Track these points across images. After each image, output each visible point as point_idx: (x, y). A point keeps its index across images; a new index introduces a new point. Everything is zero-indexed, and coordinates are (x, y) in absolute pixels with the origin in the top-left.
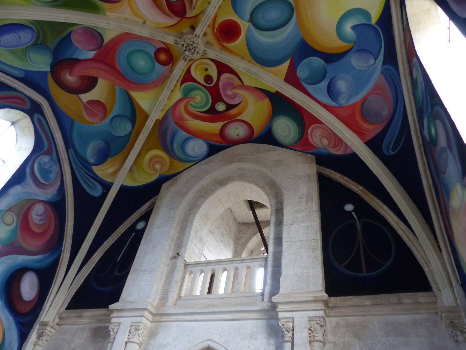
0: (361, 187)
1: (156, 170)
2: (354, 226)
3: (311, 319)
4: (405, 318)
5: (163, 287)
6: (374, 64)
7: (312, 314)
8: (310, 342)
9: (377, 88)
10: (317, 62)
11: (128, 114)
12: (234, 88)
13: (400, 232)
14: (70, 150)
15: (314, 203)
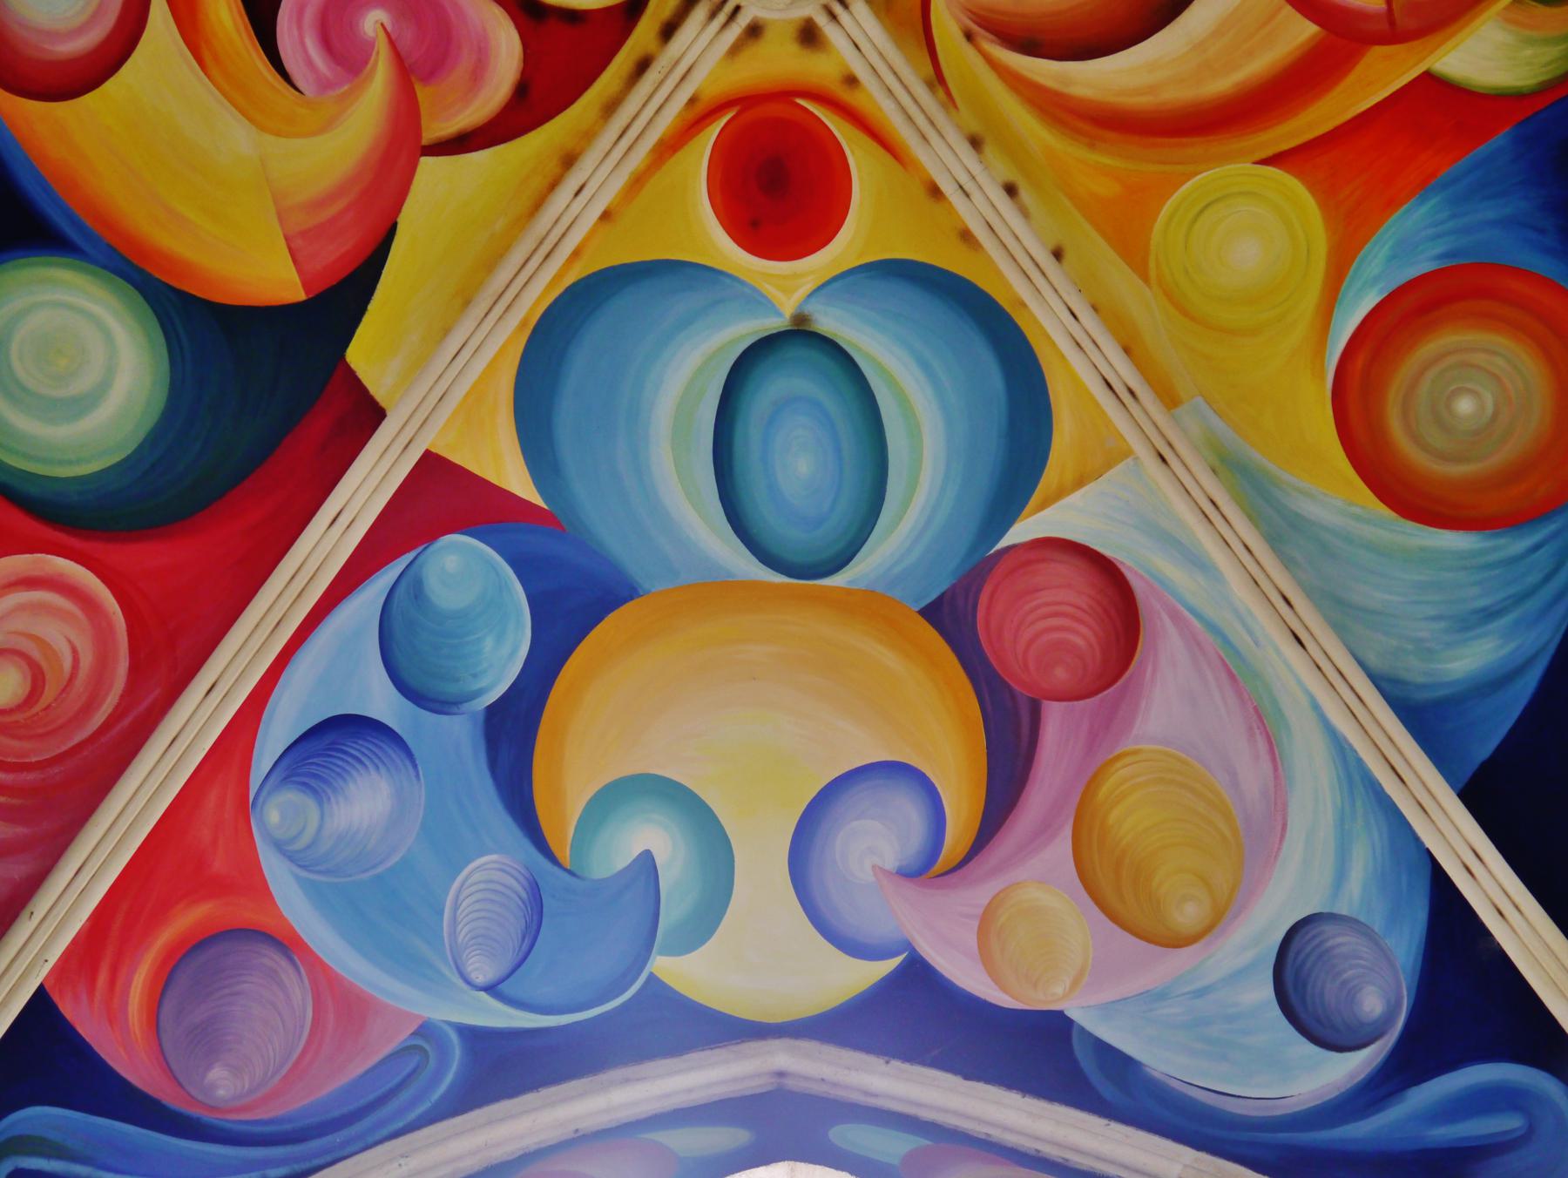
6: (468, 982)
9: (342, 1006)
12: (408, 73)
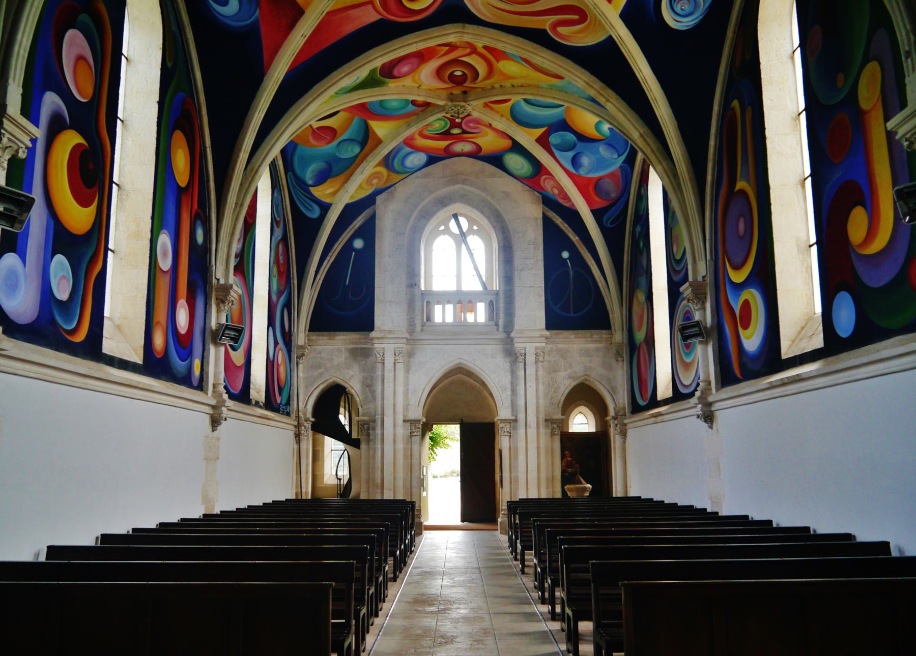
1: (372, 185)
2: (568, 273)
3: (536, 348)
4: (592, 346)
7: (538, 345)
9: (612, 175)
10: (570, 137)
11: (360, 139)
13: (600, 285)
14: (290, 173)
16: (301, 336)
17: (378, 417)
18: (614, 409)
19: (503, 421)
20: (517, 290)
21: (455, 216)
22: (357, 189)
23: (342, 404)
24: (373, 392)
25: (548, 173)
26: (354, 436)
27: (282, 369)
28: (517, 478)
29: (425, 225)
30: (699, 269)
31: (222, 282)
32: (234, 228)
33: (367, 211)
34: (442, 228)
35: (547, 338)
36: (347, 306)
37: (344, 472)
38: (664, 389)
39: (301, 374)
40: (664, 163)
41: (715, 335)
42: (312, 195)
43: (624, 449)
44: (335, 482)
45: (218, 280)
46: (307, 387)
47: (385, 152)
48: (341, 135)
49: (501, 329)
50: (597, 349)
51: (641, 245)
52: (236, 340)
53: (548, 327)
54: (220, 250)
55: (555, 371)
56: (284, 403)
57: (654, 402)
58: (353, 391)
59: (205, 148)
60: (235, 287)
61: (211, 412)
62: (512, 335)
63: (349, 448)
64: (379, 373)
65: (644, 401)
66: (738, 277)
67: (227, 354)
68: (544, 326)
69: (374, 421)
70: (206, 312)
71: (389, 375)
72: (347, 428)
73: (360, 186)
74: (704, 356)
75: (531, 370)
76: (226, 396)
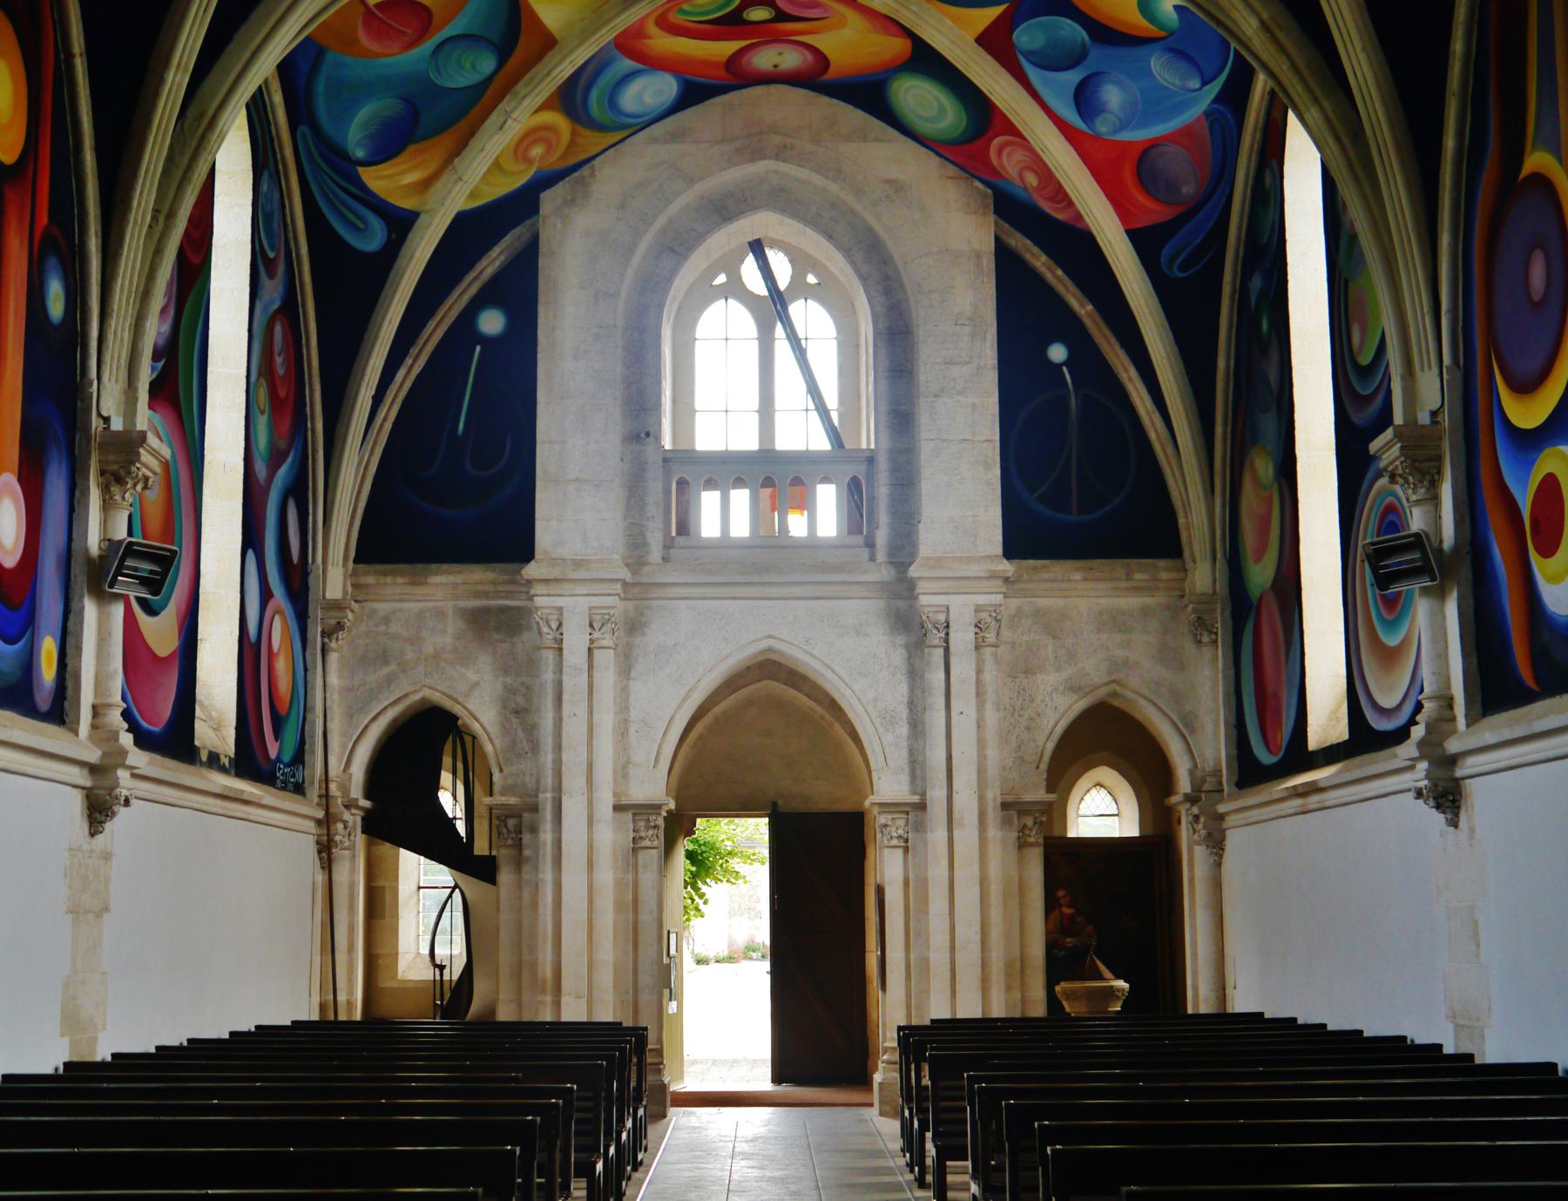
0: (1090, 307)
1: (528, 161)
5: (625, 517)
7: (982, 599)
8: (977, 648)
9: (1184, 136)
10: (1071, 30)
13: (1152, 436)
14: (303, 129)
15: (988, 344)
16: (333, 577)
17: (547, 797)
18: (1192, 773)
19: (886, 807)
20: (926, 450)
21: (757, 248)
22: (489, 171)
23: (447, 760)
24: (531, 730)
25: (1012, 130)
26: (481, 848)
27: (281, 666)
28: (925, 963)
29: (673, 272)
30: (1423, 391)
31: (117, 425)
32: (150, 278)
33: (518, 230)
34: (721, 279)
35: (1006, 580)
36: (459, 494)
37: (452, 949)
38: (1326, 717)
39: (333, 679)
40: (1326, 104)
41: (1466, 572)
42: (363, 187)
43: (1217, 885)
44: (427, 974)
45: (107, 420)
46: (350, 716)
47: (565, 70)
48: (442, 27)
49: (881, 556)
50: (1145, 612)
51: (1265, 325)
52: (154, 584)
53: (1012, 550)
54: (110, 337)
55: (1028, 672)
56: (287, 758)
57: (1299, 757)
58: (476, 727)
59: (70, 56)
60: (152, 440)
61: (88, 783)
62: (913, 572)
63: (467, 882)
64: (548, 676)
65: (1270, 750)
66: (1528, 413)
67: (130, 622)
68: (999, 550)
69: (535, 809)
70: (71, 509)
71: (574, 683)
72: (461, 827)
73: (496, 164)
74: (1436, 629)
75: (963, 668)
76: (127, 739)
